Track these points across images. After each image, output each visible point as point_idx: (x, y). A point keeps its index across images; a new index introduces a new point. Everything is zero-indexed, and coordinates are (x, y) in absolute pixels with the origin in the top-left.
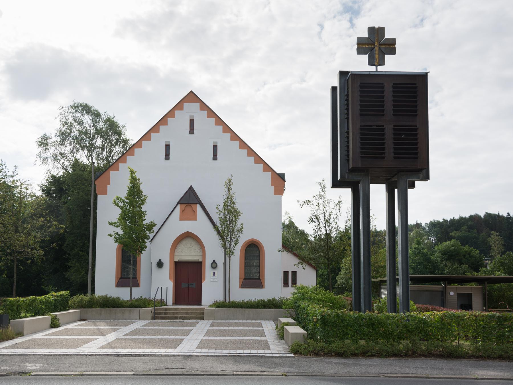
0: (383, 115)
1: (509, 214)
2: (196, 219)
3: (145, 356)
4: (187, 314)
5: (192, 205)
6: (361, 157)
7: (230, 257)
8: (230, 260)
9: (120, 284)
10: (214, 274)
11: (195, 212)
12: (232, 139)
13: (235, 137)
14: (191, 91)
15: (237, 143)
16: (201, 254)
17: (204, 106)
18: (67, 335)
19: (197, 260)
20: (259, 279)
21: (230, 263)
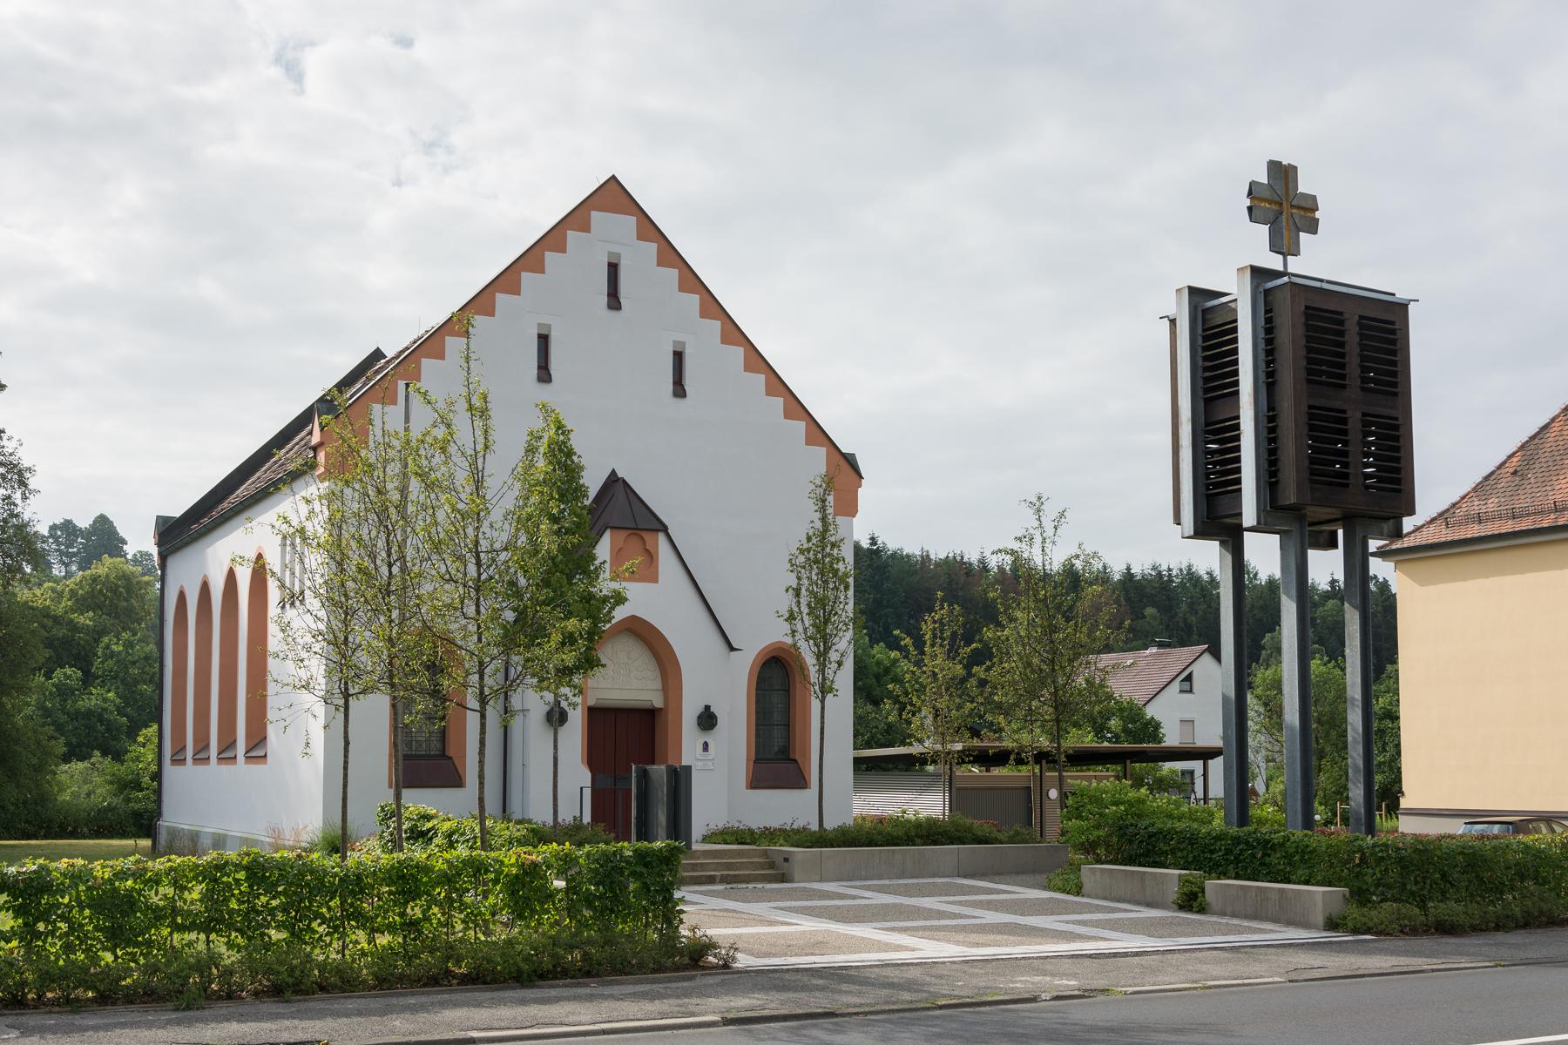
0: (1344, 387)
1: (873, 540)
2: (655, 580)
3: (1126, 955)
4: (729, 866)
5: (644, 534)
6: (1312, 482)
7: (822, 702)
8: (823, 708)
9: (758, 781)
10: (706, 747)
11: (651, 557)
12: (726, 340)
13: (733, 334)
14: (613, 177)
15: (739, 352)
16: (658, 685)
17: (649, 229)
18: (839, 907)
19: (647, 705)
20: (443, 755)
21: (822, 717)
